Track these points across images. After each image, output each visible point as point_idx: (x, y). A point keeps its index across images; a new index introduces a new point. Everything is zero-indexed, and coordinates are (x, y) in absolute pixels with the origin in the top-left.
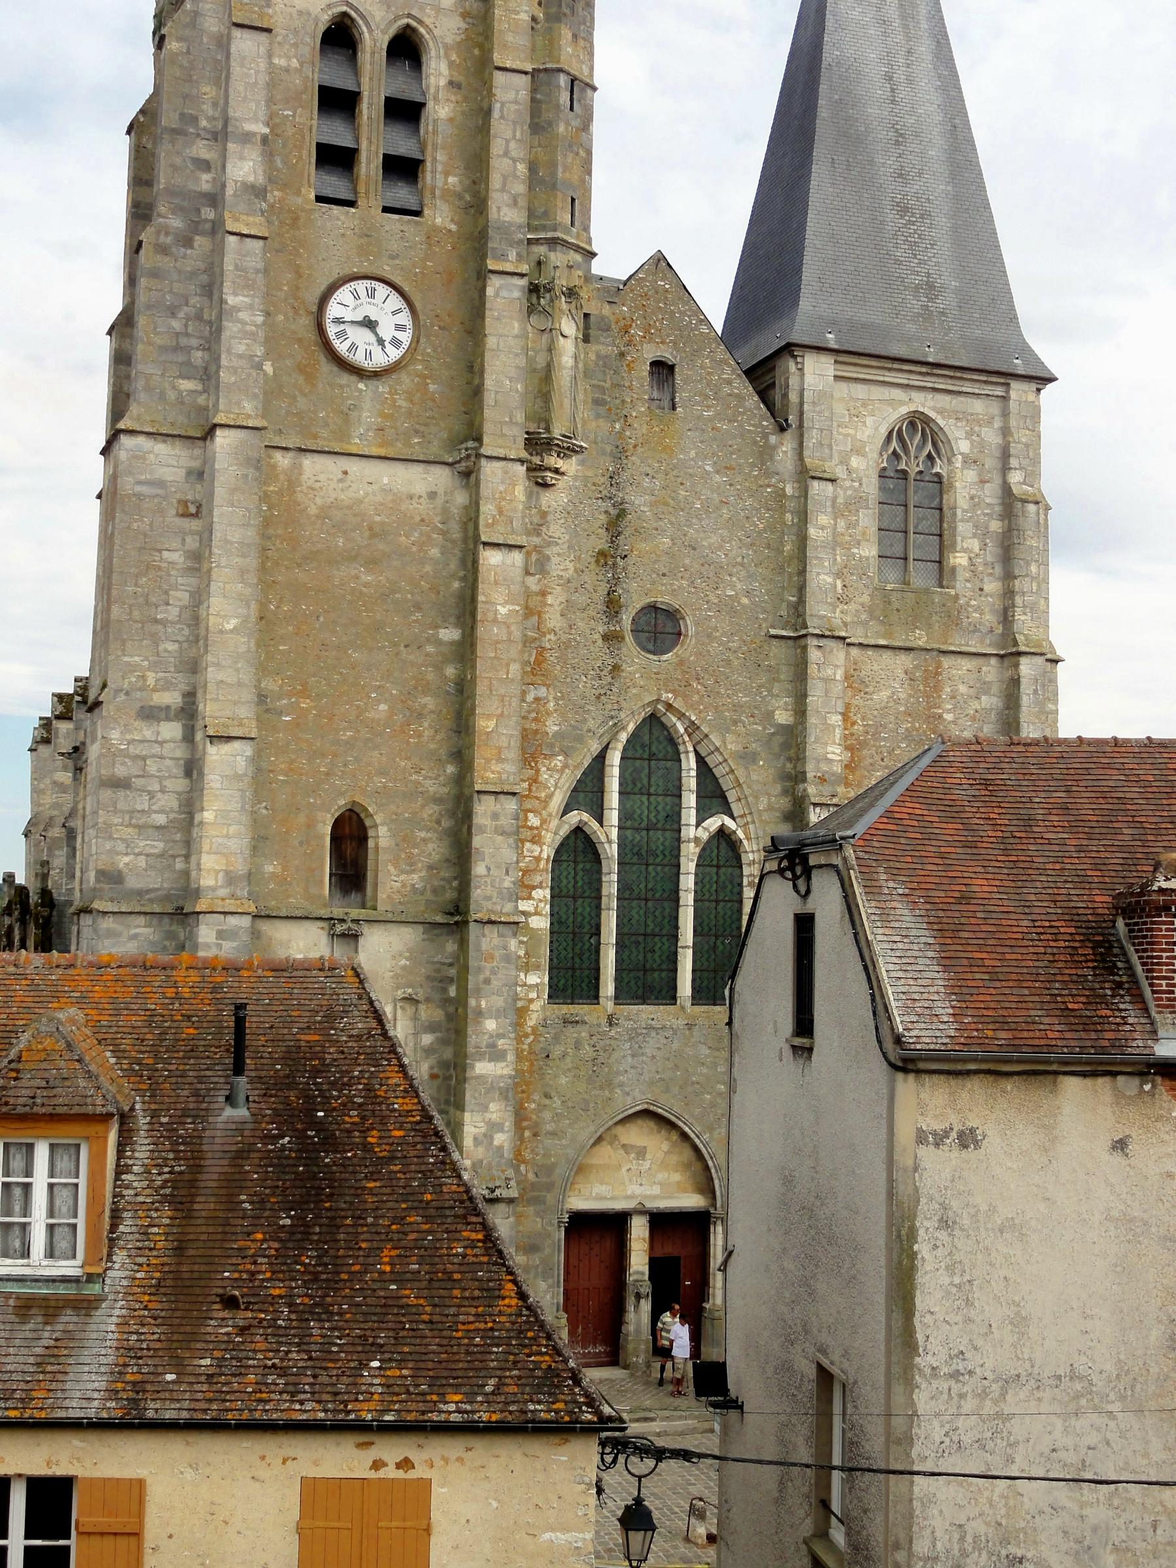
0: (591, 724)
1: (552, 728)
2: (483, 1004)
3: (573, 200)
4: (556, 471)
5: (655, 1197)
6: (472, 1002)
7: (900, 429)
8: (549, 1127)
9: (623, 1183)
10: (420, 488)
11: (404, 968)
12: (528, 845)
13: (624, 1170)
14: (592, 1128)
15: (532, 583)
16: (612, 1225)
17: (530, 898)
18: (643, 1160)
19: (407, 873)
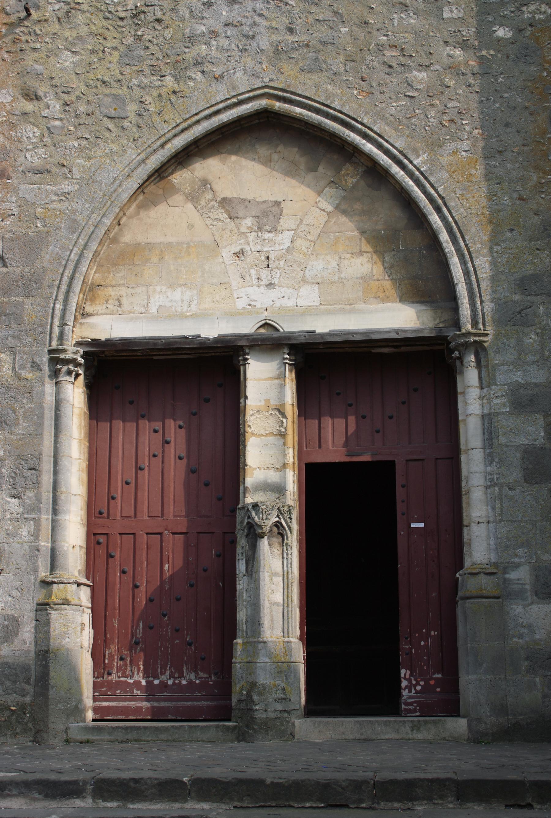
5: (307, 312)
8: (33, 159)
13: (227, 253)
14: (132, 154)
16: (201, 374)
18: (274, 230)
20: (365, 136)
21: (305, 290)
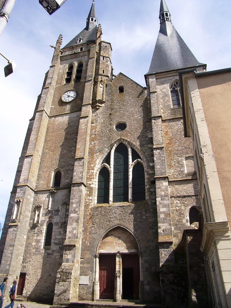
0: (105, 145)
1: (97, 148)
2: (73, 201)
3: (103, 71)
4: (99, 106)
6: (71, 201)
7: (174, 84)
9: (114, 247)
10: (75, 116)
11: (64, 199)
12: (91, 171)
15: (94, 125)
17: (91, 181)
19: (67, 179)
20: (129, 229)
21: (123, 247)
